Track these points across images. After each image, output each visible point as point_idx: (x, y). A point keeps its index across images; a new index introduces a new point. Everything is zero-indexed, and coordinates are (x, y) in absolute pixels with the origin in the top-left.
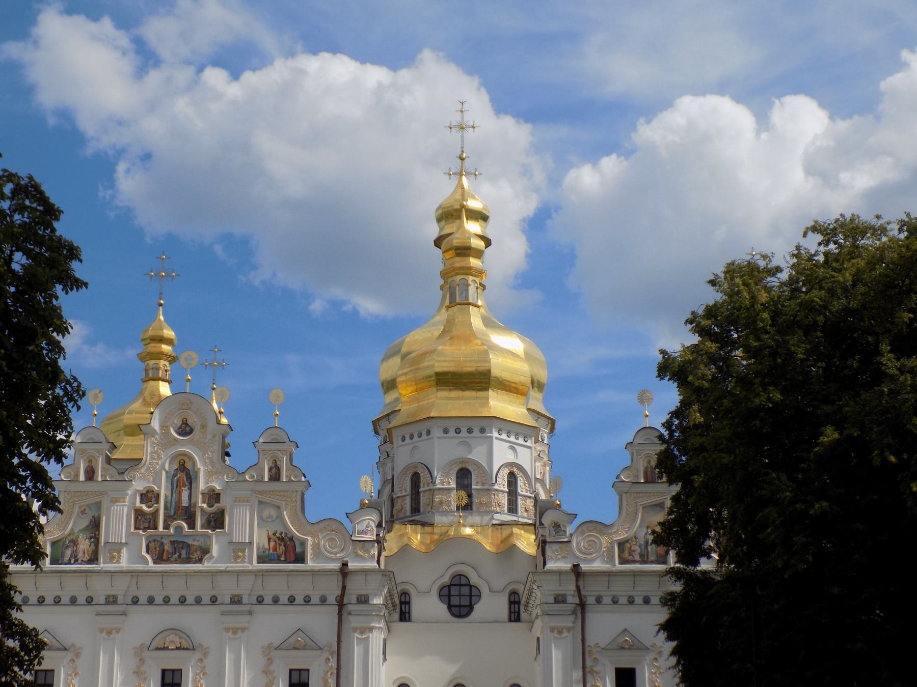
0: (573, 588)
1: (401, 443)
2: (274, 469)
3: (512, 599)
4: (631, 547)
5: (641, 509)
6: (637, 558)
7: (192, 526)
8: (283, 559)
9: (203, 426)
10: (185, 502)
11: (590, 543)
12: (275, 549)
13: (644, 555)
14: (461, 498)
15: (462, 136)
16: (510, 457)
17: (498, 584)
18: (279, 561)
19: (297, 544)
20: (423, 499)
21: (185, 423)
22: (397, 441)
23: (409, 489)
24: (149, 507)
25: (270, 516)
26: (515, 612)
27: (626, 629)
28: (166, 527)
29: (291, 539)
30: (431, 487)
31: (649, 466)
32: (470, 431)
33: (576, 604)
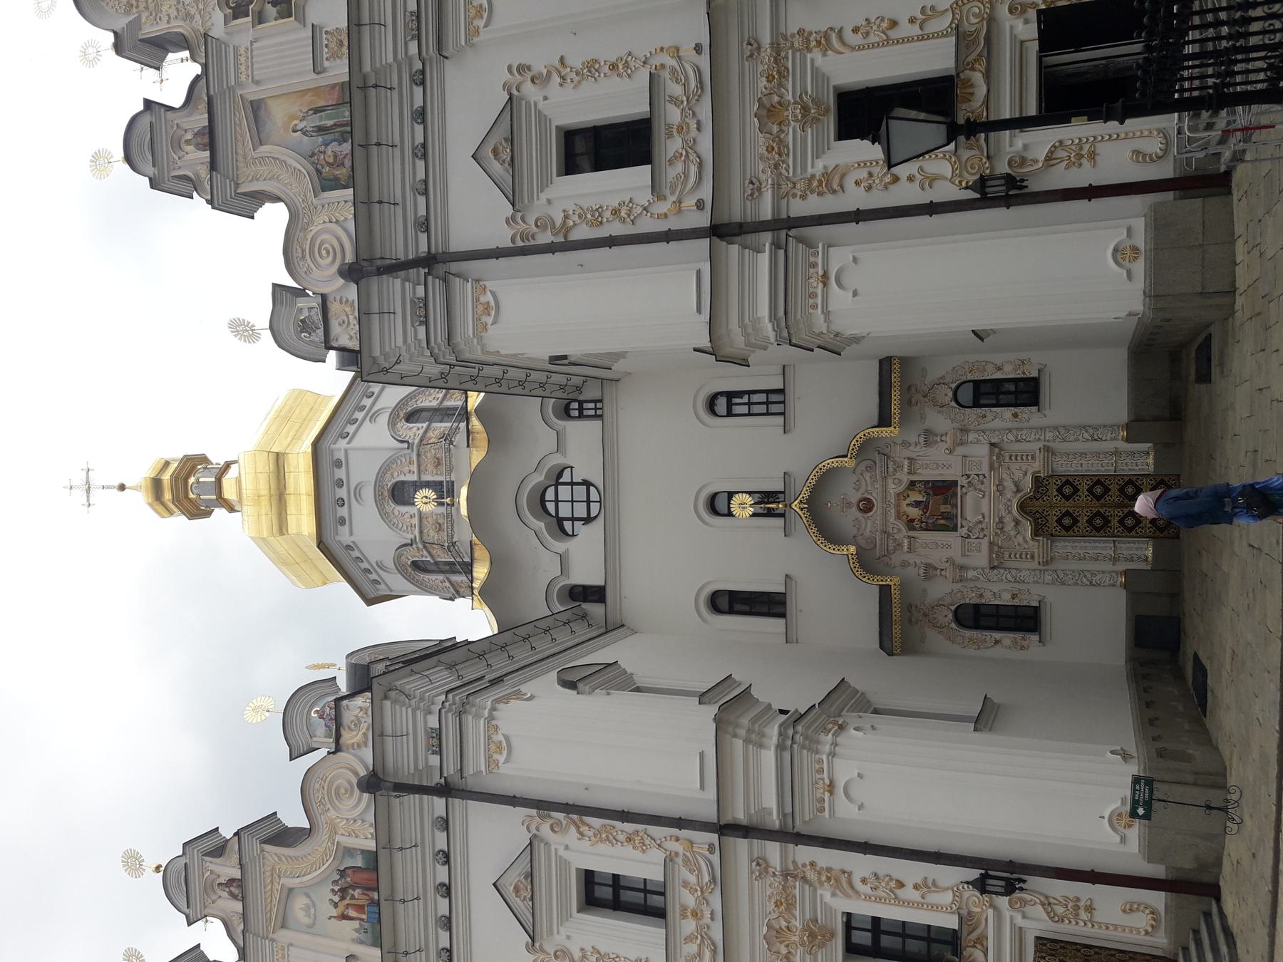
0: (398, 281)
1: (383, 586)
3: (576, 413)
5: (262, 149)
11: (324, 252)
13: (342, 133)
14: (425, 500)
16: (384, 419)
17: (546, 439)
20: (444, 557)
22: (383, 590)
23: (441, 577)
26: (596, 409)
30: (421, 546)
31: (194, 141)
32: (340, 483)
33: (426, 275)
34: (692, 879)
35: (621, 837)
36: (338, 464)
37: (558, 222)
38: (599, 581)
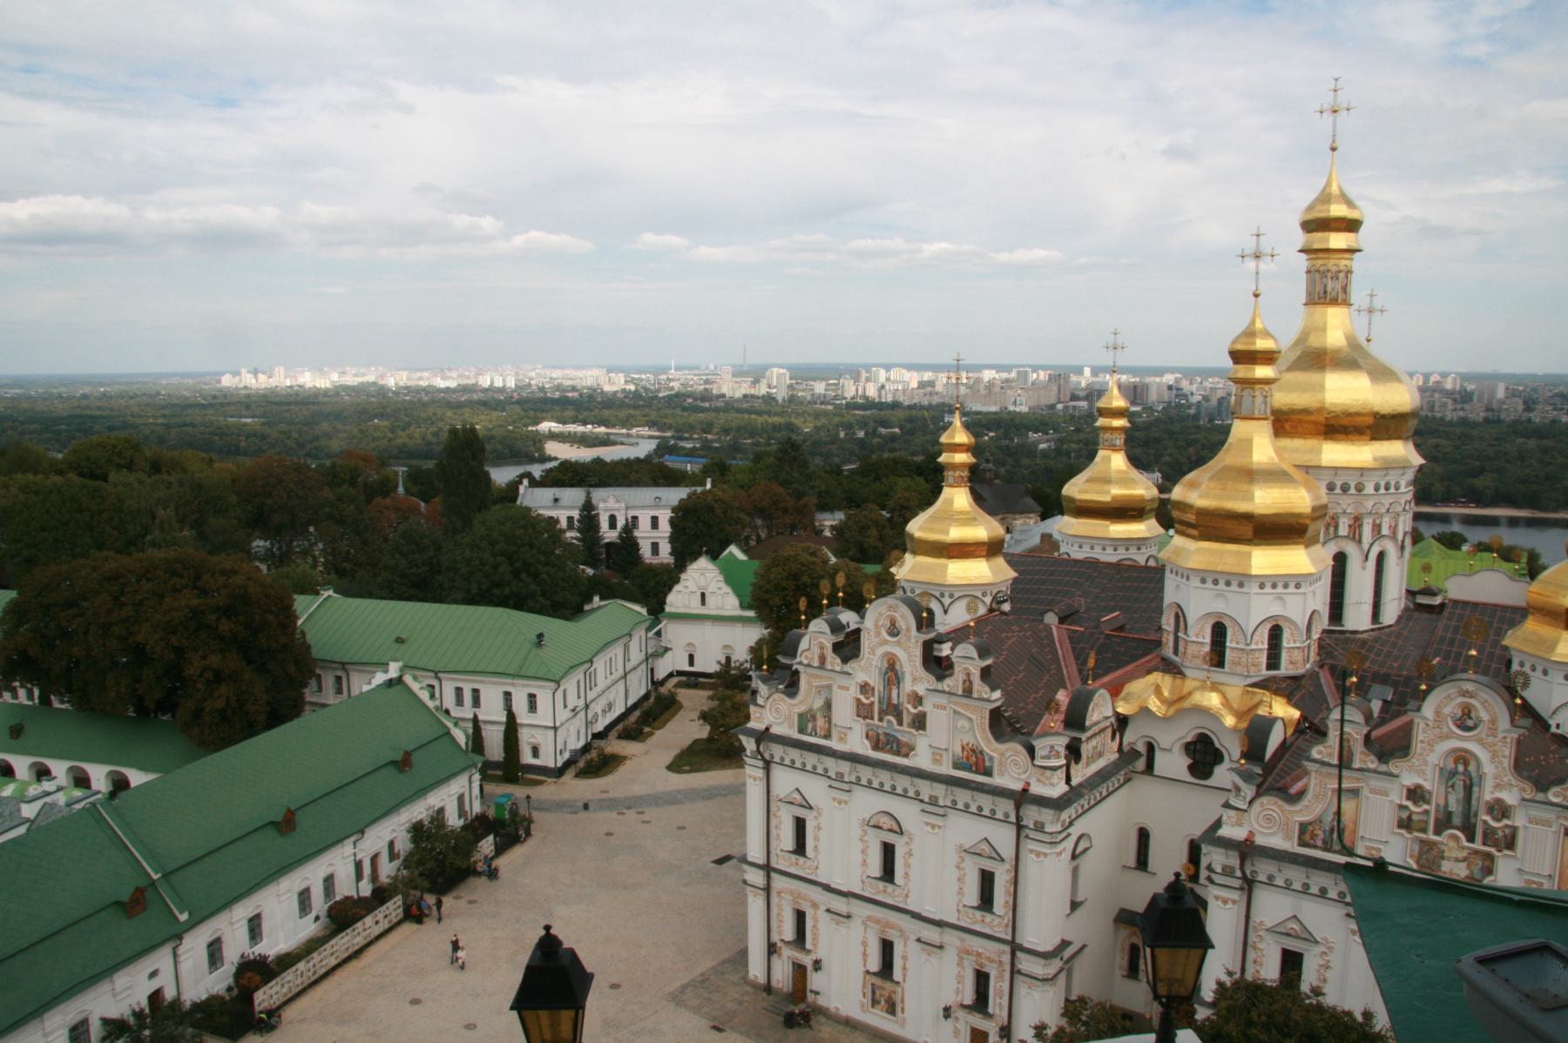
2: (967, 683)
4: (1312, 832)
6: (1319, 843)
7: (900, 723)
8: (974, 769)
9: (908, 630)
10: (895, 701)
12: (968, 758)
15: (1335, 126)
16: (1275, 609)
18: (971, 771)
19: (987, 759)
20: (1181, 644)
21: (893, 623)
24: (868, 699)
25: (963, 727)
27: (1295, 917)
28: (881, 720)
29: (981, 752)
32: (1228, 584)
34: (995, 923)
35: (1008, 899)
36: (1241, 585)
37: (1259, 945)
38: (1158, 770)
